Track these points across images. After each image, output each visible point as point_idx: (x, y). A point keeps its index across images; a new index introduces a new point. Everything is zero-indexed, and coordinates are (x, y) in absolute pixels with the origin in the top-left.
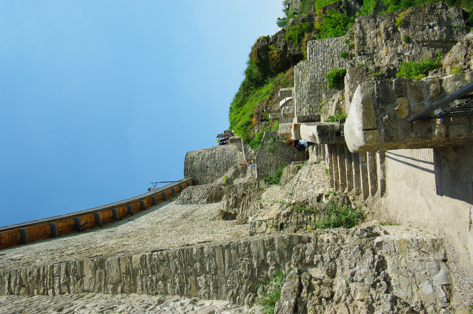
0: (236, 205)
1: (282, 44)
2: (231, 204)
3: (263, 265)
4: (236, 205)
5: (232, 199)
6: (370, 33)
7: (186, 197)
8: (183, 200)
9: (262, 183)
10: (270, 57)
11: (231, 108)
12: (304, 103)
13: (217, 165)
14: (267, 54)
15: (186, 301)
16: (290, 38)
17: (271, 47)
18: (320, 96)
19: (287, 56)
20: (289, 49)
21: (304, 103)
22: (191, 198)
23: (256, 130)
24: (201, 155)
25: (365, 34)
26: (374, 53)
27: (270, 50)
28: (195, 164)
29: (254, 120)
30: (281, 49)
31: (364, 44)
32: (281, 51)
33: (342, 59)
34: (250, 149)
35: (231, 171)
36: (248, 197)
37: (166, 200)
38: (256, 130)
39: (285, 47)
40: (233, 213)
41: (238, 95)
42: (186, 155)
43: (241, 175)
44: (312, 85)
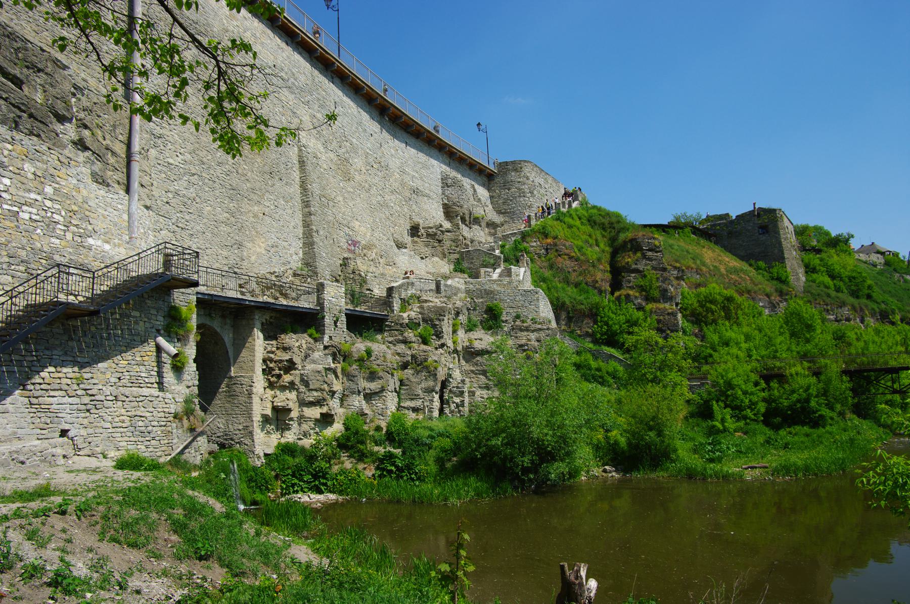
0: (428, 235)
1: (640, 267)
2: (430, 230)
3: (311, 266)
4: (428, 235)
5: (434, 230)
6: (533, 336)
7: (450, 181)
8: (446, 179)
9: (457, 256)
10: (627, 253)
11: (594, 207)
12: (477, 286)
13: (511, 200)
14: (631, 250)
15: (301, 245)
16: (645, 276)
17: (639, 254)
18: (482, 298)
19: (623, 274)
20: (633, 275)
21: (477, 286)
22: (448, 187)
23: (534, 244)
24: (525, 179)
25: (533, 331)
26: (511, 336)
27: (635, 253)
28: (513, 174)
29: (549, 241)
30: (634, 266)
31: (521, 330)
32: (631, 266)
33: (515, 315)
34: (513, 239)
35: (498, 219)
36: (436, 244)
37: (450, 157)
38: (534, 244)
39: (637, 271)
40: (420, 234)
41: (608, 214)
42: (525, 161)
43: (493, 231)
44: (492, 292)
